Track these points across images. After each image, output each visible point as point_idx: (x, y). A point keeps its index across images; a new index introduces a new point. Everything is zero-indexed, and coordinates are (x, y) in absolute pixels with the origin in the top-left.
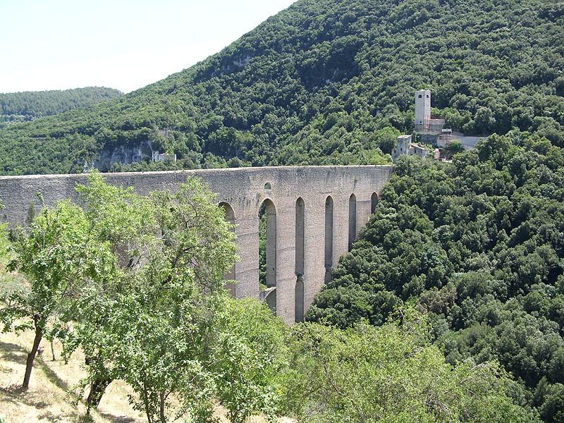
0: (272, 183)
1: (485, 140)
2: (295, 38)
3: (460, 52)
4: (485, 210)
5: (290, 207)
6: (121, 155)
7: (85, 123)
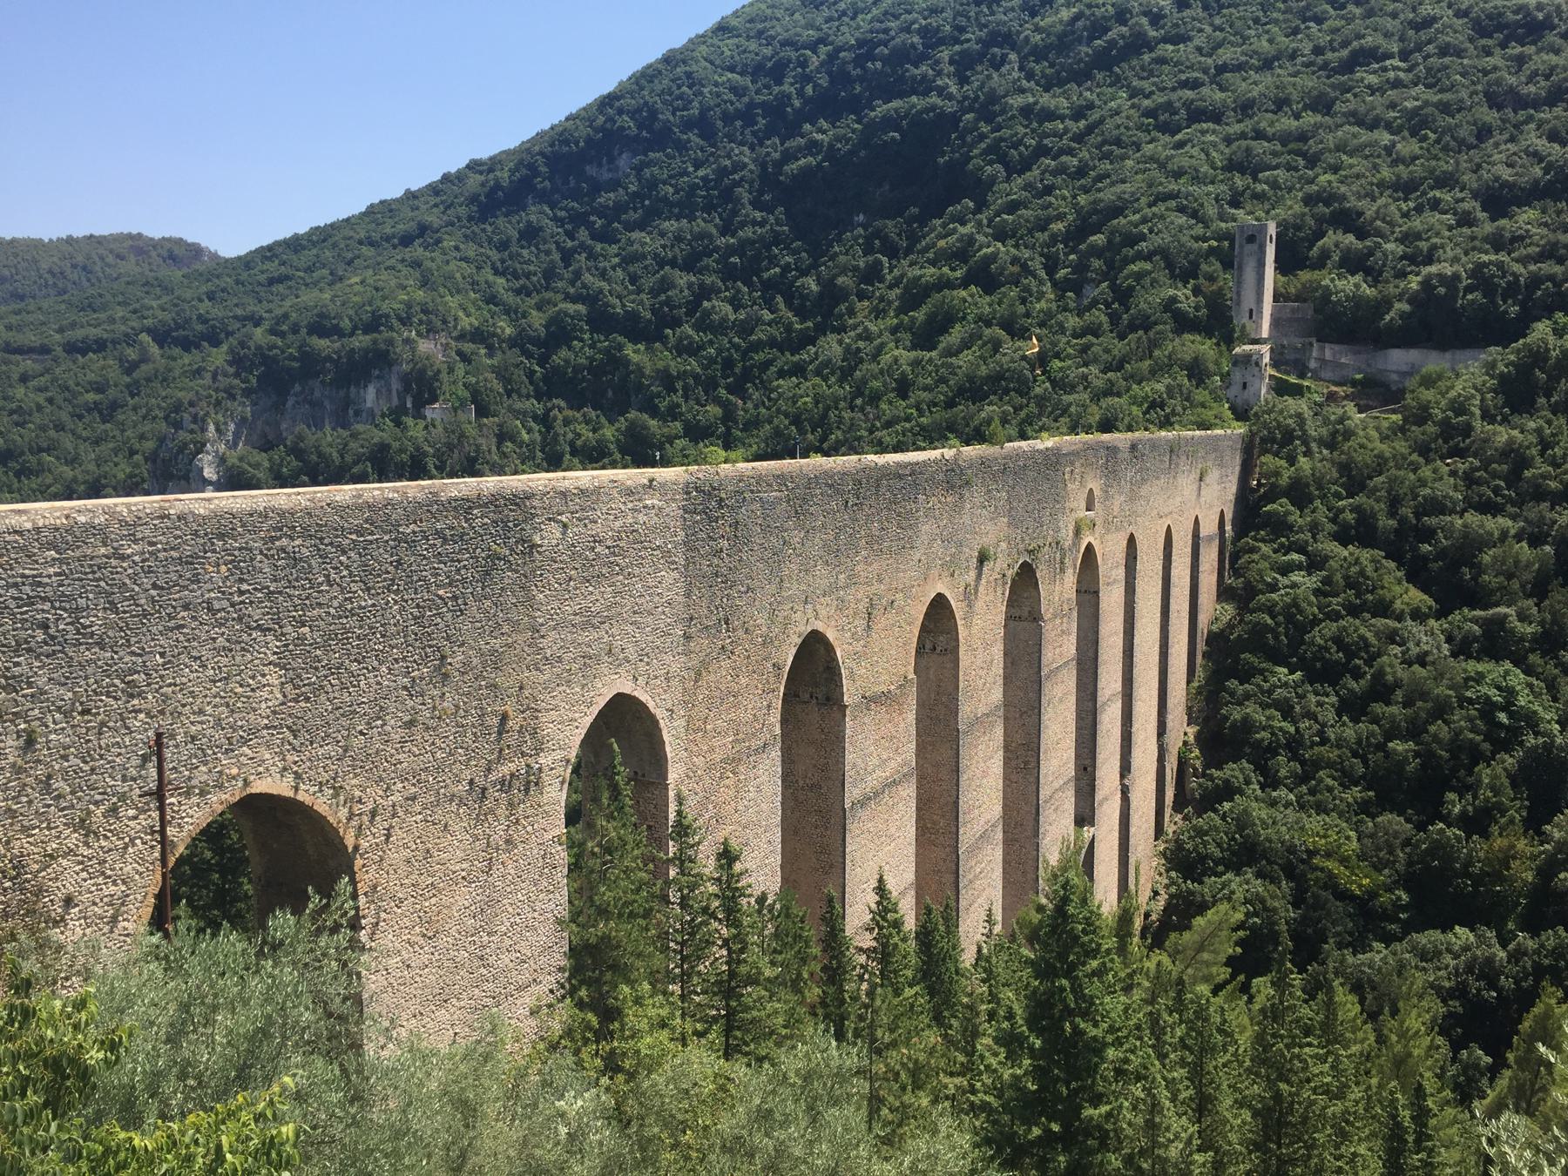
2: (751, 105)
3: (1287, 123)
6: (312, 404)
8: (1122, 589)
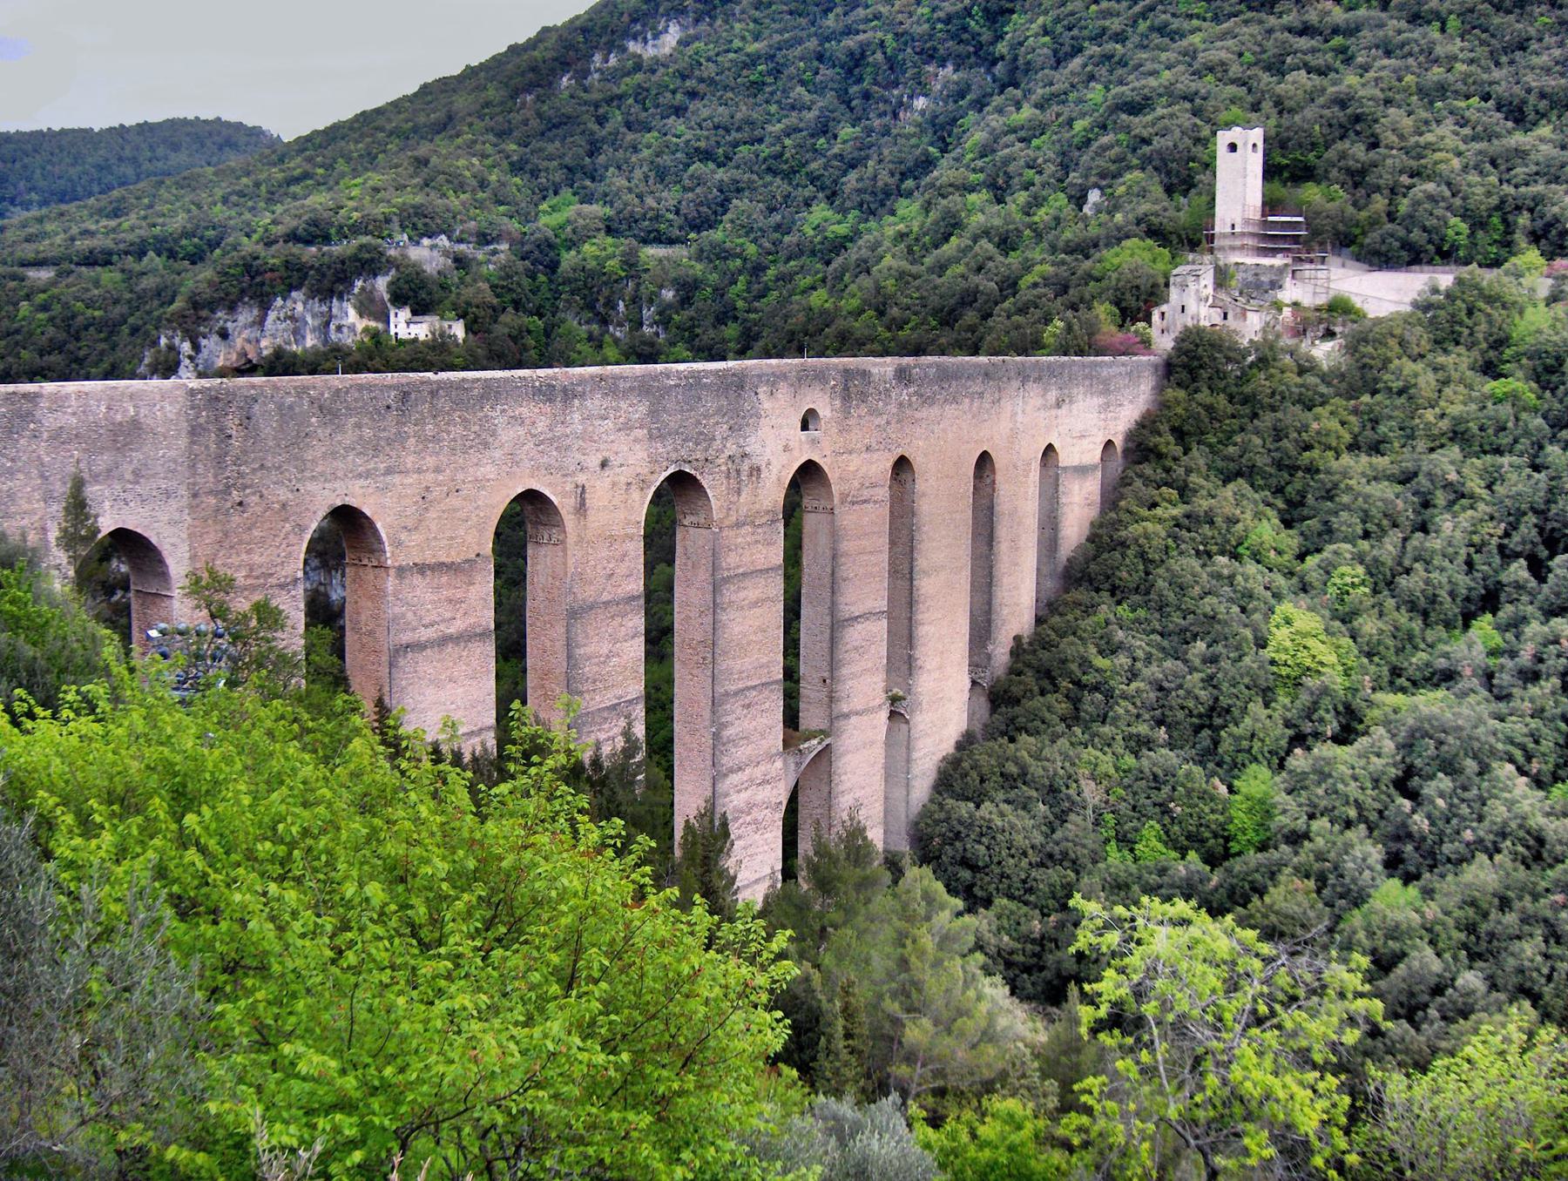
0: (824, 412)
1: (1445, 279)
4: (1458, 495)
5: (873, 486)
6: (292, 318)
7: (178, 222)
8: (885, 511)
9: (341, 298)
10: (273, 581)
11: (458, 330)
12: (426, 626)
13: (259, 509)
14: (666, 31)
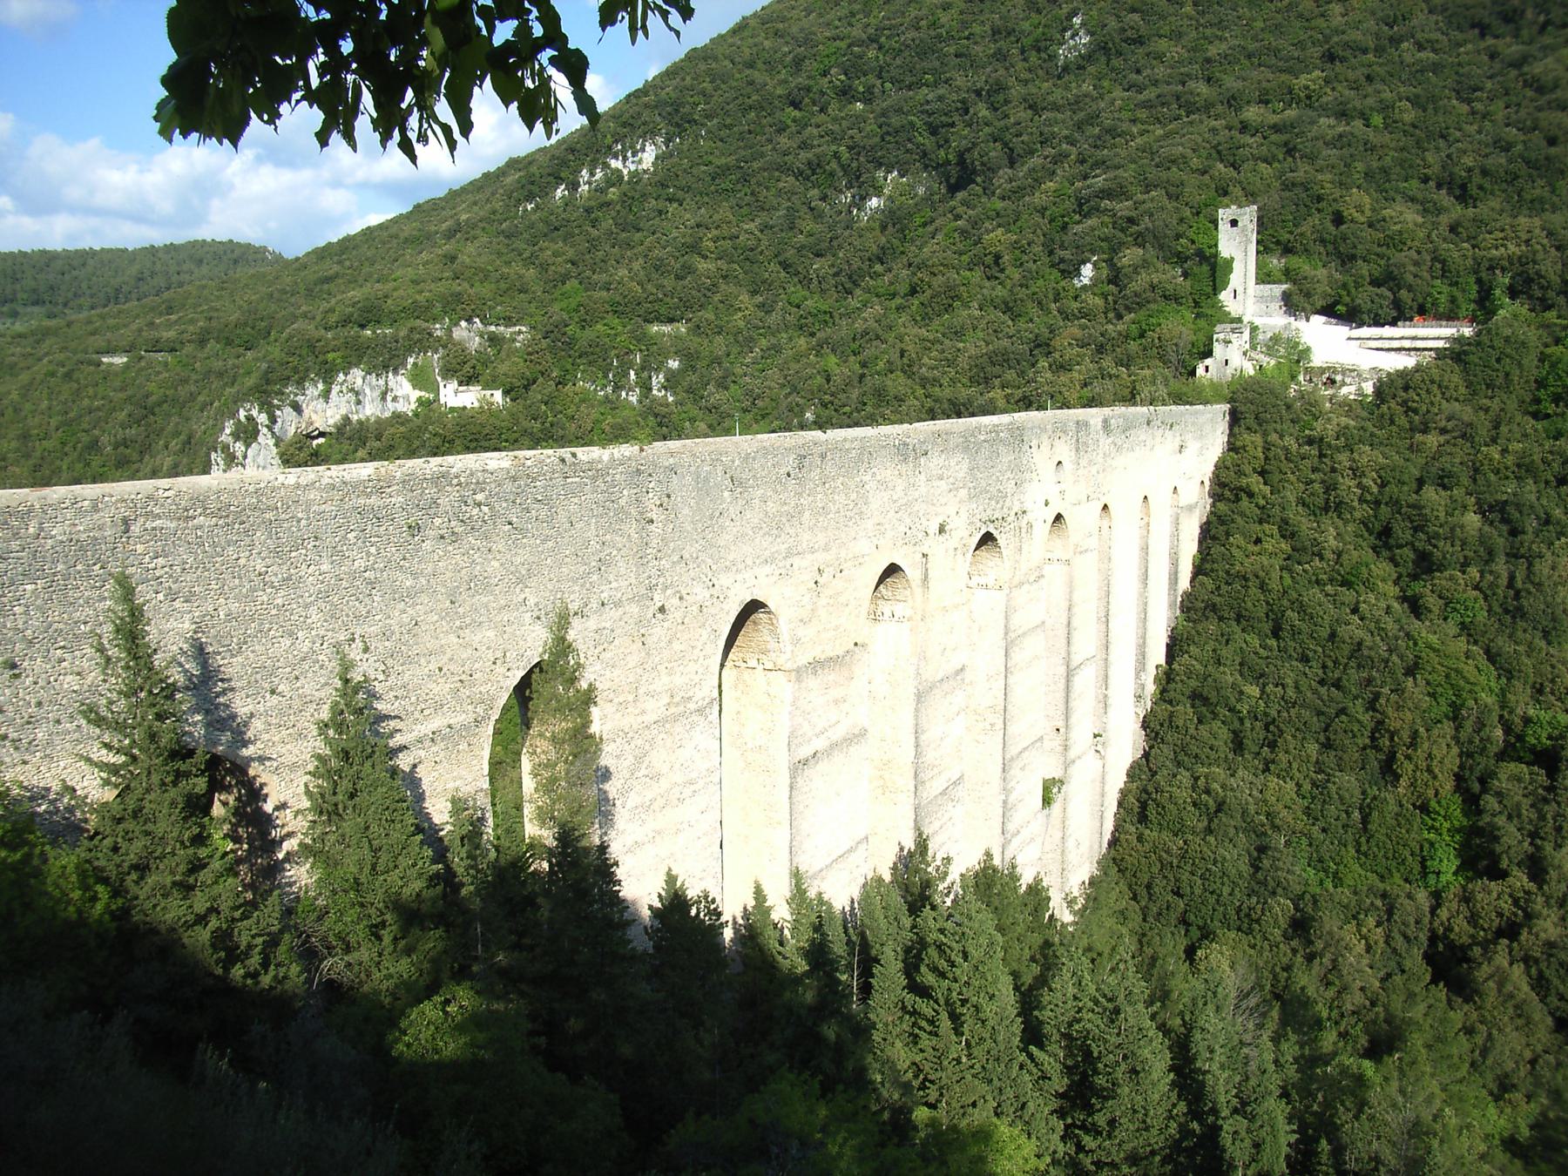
9: (396, 372)
10: (692, 706)
11: (498, 396)
12: (817, 736)
13: (678, 615)
14: (643, 150)
